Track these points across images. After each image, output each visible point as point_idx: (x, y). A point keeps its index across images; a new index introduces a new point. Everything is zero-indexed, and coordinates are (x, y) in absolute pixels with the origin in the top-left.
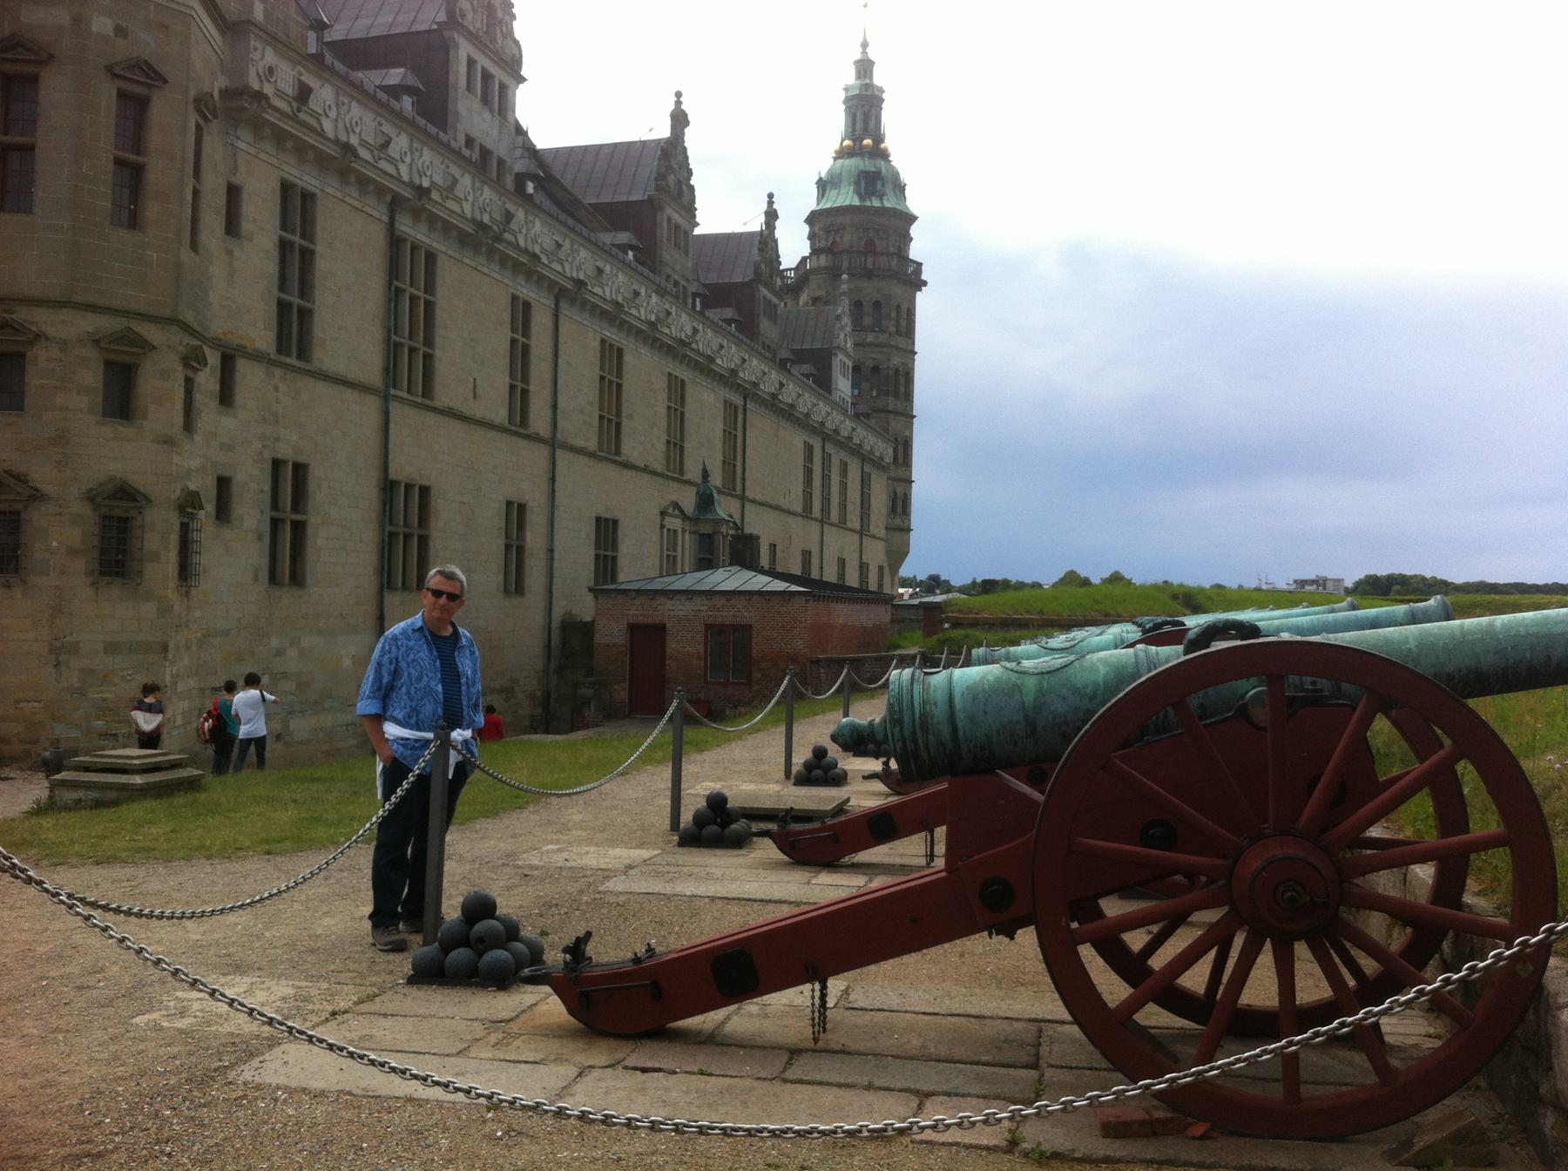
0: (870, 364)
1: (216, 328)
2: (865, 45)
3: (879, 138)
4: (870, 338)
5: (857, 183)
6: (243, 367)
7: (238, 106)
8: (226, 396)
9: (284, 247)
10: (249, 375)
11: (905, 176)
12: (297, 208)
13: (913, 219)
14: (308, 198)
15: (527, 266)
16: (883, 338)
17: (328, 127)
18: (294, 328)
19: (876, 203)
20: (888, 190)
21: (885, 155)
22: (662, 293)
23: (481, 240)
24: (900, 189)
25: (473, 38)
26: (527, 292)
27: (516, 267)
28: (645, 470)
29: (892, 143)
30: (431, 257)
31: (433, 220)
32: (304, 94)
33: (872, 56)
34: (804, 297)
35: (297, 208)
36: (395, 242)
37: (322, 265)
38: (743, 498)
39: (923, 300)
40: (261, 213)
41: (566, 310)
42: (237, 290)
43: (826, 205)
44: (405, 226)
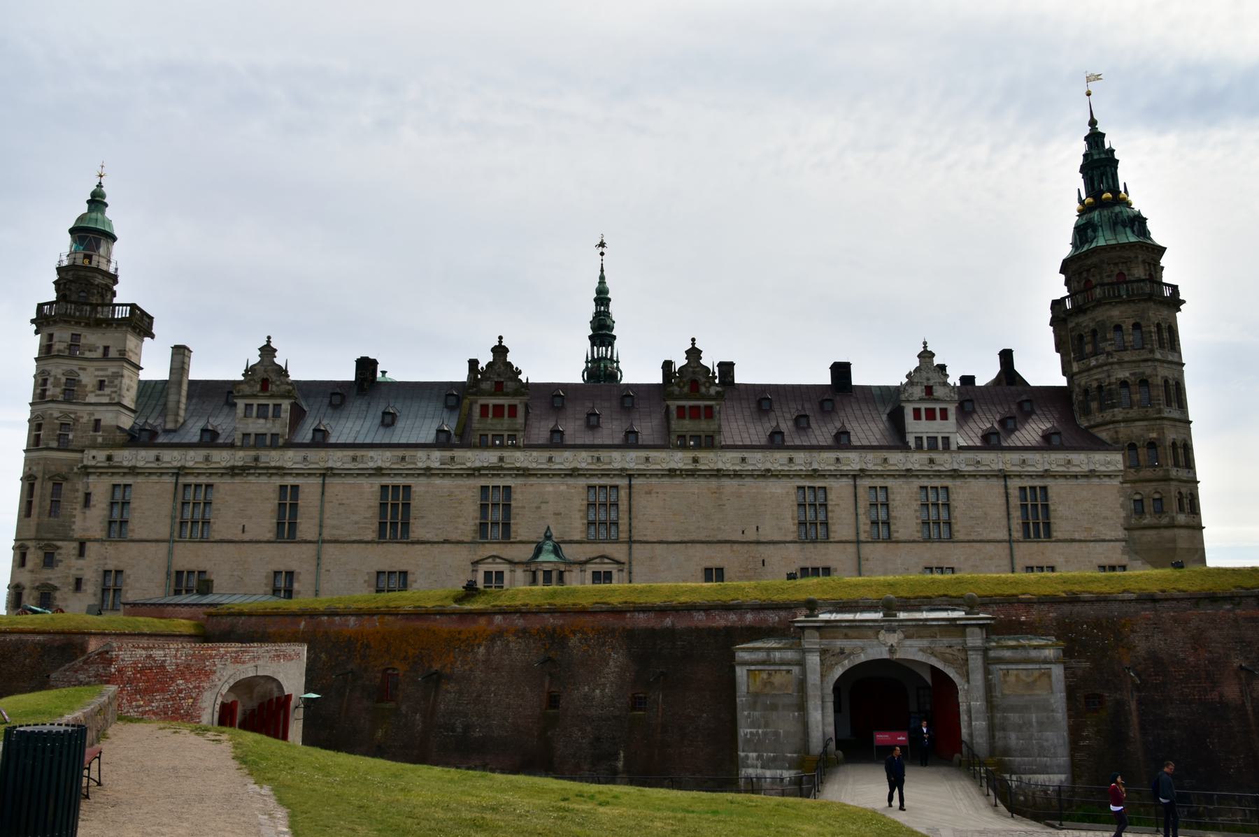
0: (1095, 384)
1: (78, 534)
6: (88, 544)
7: (86, 471)
8: (81, 554)
10: (92, 548)
15: (280, 471)
16: (1102, 358)
17: (125, 464)
18: (117, 527)
23: (233, 471)
28: (446, 542)
38: (630, 542)
42: (91, 522)
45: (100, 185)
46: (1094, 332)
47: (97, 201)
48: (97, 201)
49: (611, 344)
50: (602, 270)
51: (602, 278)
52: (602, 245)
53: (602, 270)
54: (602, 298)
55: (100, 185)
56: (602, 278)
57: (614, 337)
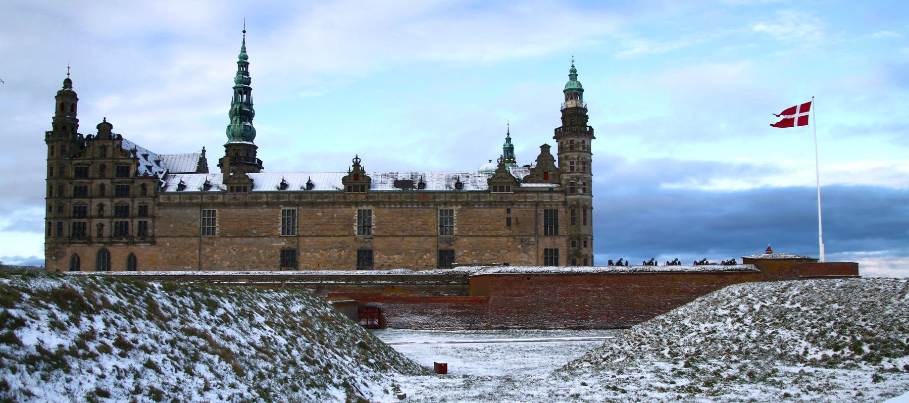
45: (573, 66)
47: (573, 74)
55: (573, 66)
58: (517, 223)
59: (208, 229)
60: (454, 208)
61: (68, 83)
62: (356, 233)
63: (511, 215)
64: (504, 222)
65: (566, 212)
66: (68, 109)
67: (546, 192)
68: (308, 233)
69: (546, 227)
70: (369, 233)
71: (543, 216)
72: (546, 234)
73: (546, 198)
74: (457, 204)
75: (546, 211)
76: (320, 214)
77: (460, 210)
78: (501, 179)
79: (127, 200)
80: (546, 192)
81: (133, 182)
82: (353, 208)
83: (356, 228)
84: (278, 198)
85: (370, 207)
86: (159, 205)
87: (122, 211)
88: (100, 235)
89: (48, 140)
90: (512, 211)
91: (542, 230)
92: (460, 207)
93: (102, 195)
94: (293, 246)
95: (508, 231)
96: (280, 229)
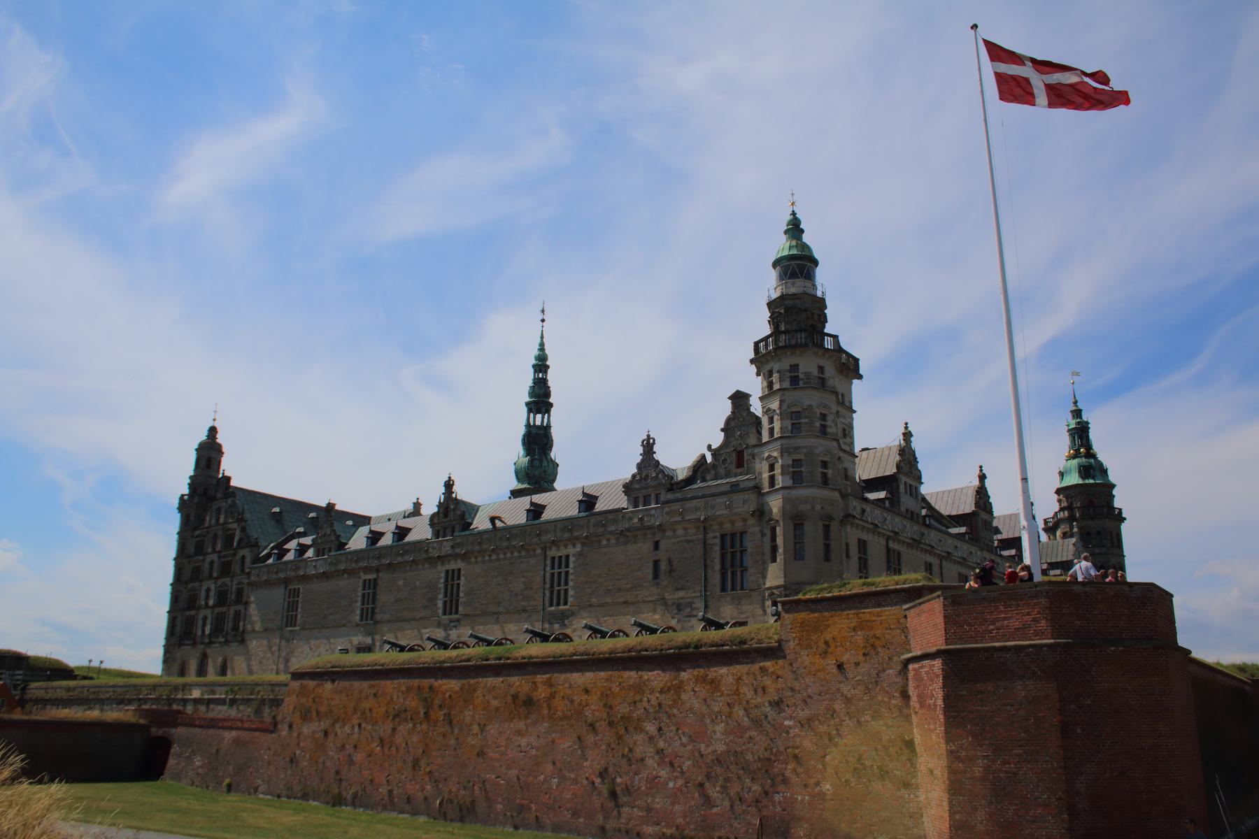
2: (1075, 403)
3: (1088, 447)
4: (1097, 551)
5: (1080, 472)
9: (860, 558)
11: (1106, 463)
12: (862, 544)
13: (1113, 486)
14: (865, 542)
15: (930, 550)
19: (1092, 481)
20: (1098, 473)
21: (1094, 456)
22: (982, 550)
24: (1104, 472)
25: (906, 475)
26: (930, 559)
27: (926, 551)
29: (1097, 447)
30: (899, 553)
31: (899, 541)
32: (863, 511)
33: (1080, 406)
34: (1059, 533)
35: (862, 544)
36: (888, 549)
37: (870, 562)
39: (1124, 527)
40: (854, 550)
41: (944, 562)
43: (1065, 484)
44: (891, 544)
45: (794, 214)
46: (1099, 533)
47: (795, 229)
48: (795, 229)
49: (548, 411)
50: (542, 337)
51: (542, 347)
52: (543, 311)
53: (542, 337)
54: (541, 366)
55: (794, 214)
56: (542, 347)
57: (551, 405)
58: (671, 570)
59: (291, 621)
60: (571, 551)
61: (213, 431)
62: (440, 612)
63: (662, 555)
64: (649, 571)
65: (763, 535)
66: (204, 463)
67: (723, 494)
68: (386, 617)
69: (723, 575)
70: (457, 613)
71: (717, 548)
72: (723, 589)
73: (720, 509)
74: (573, 541)
75: (723, 537)
76: (401, 583)
77: (580, 554)
78: (650, 479)
79: (227, 580)
80: (723, 494)
81: (235, 555)
82: (440, 568)
83: (440, 604)
84: (356, 561)
85: (459, 564)
86: (250, 584)
87: (222, 598)
88: (203, 631)
89: (180, 509)
90: (662, 545)
91: (716, 579)
92: (578, 548)
93: (210, 577)
94: (369, 641)
95: (655, 590)
96: (358, 612)
